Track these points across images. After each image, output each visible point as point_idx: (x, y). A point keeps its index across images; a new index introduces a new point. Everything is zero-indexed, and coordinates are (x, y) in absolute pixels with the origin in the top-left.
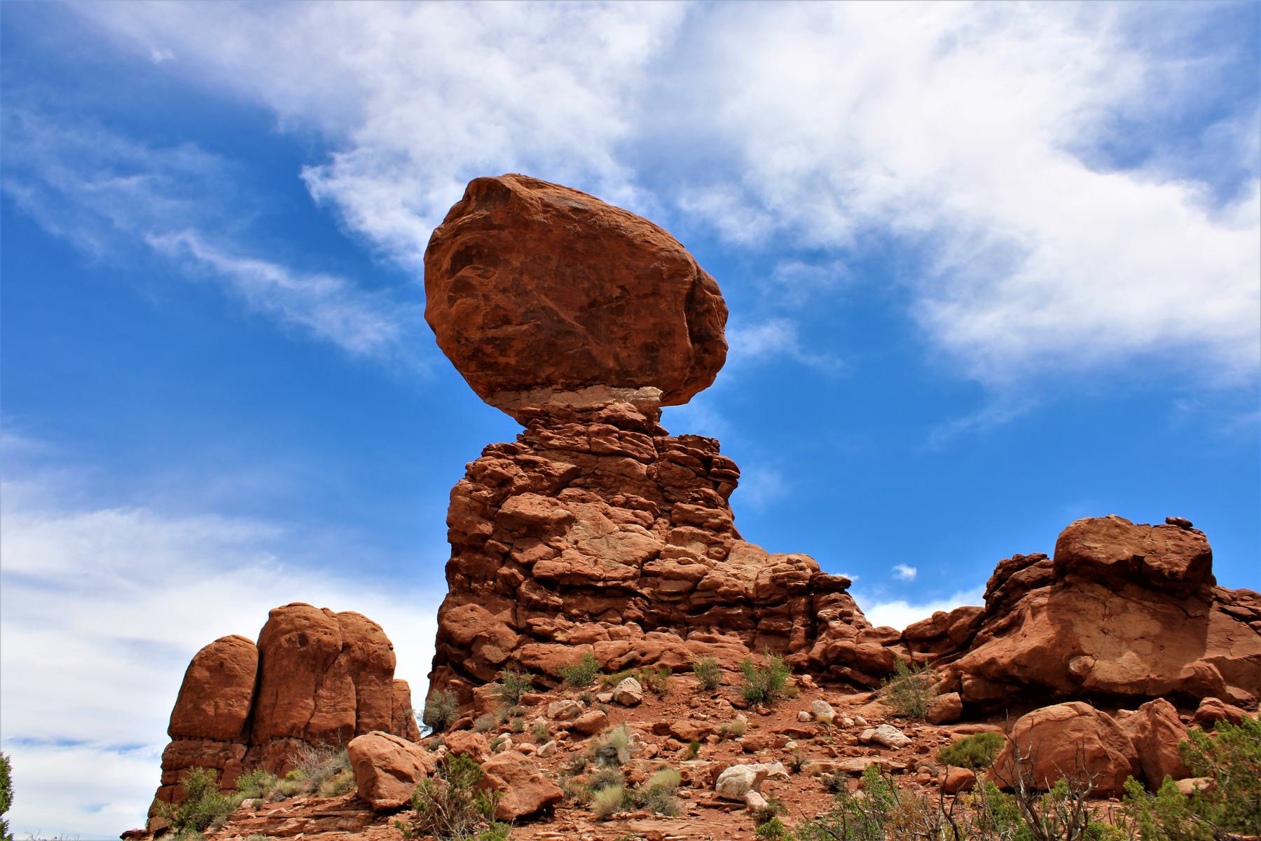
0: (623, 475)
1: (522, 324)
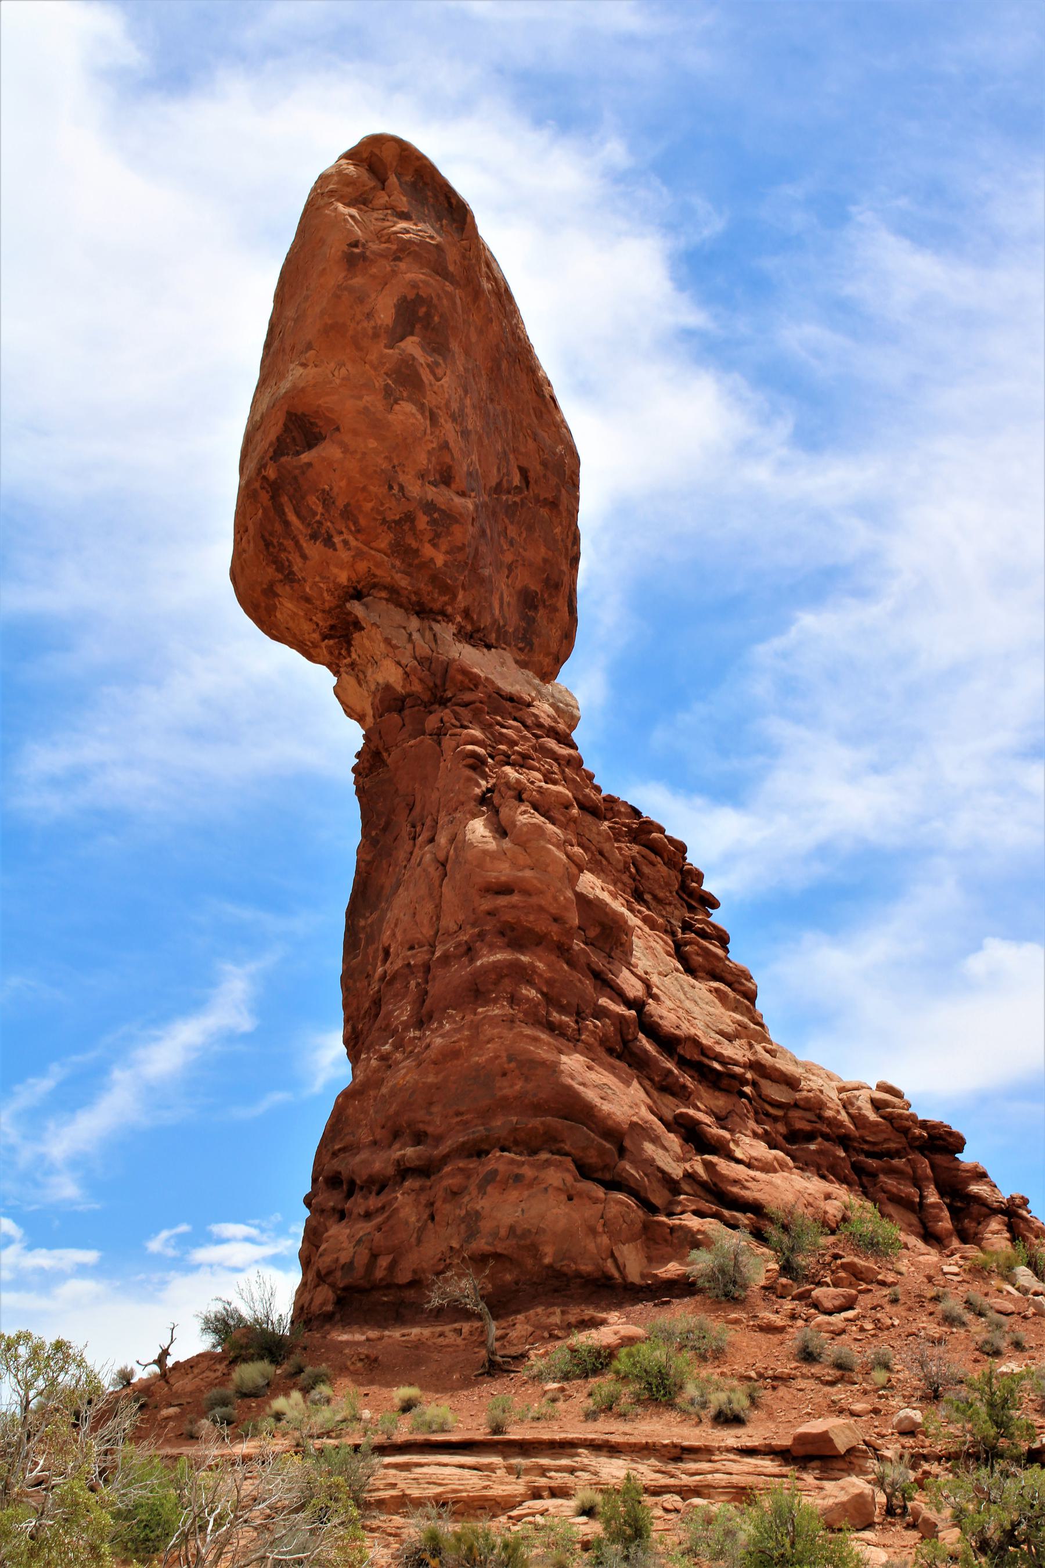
0: (601, 853)
1: (463, 494)
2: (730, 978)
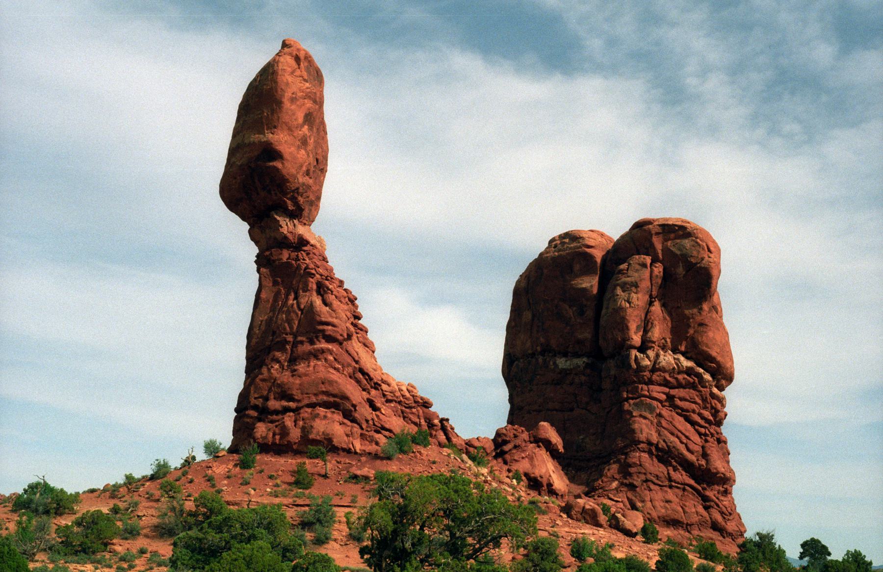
2: (368, 345)
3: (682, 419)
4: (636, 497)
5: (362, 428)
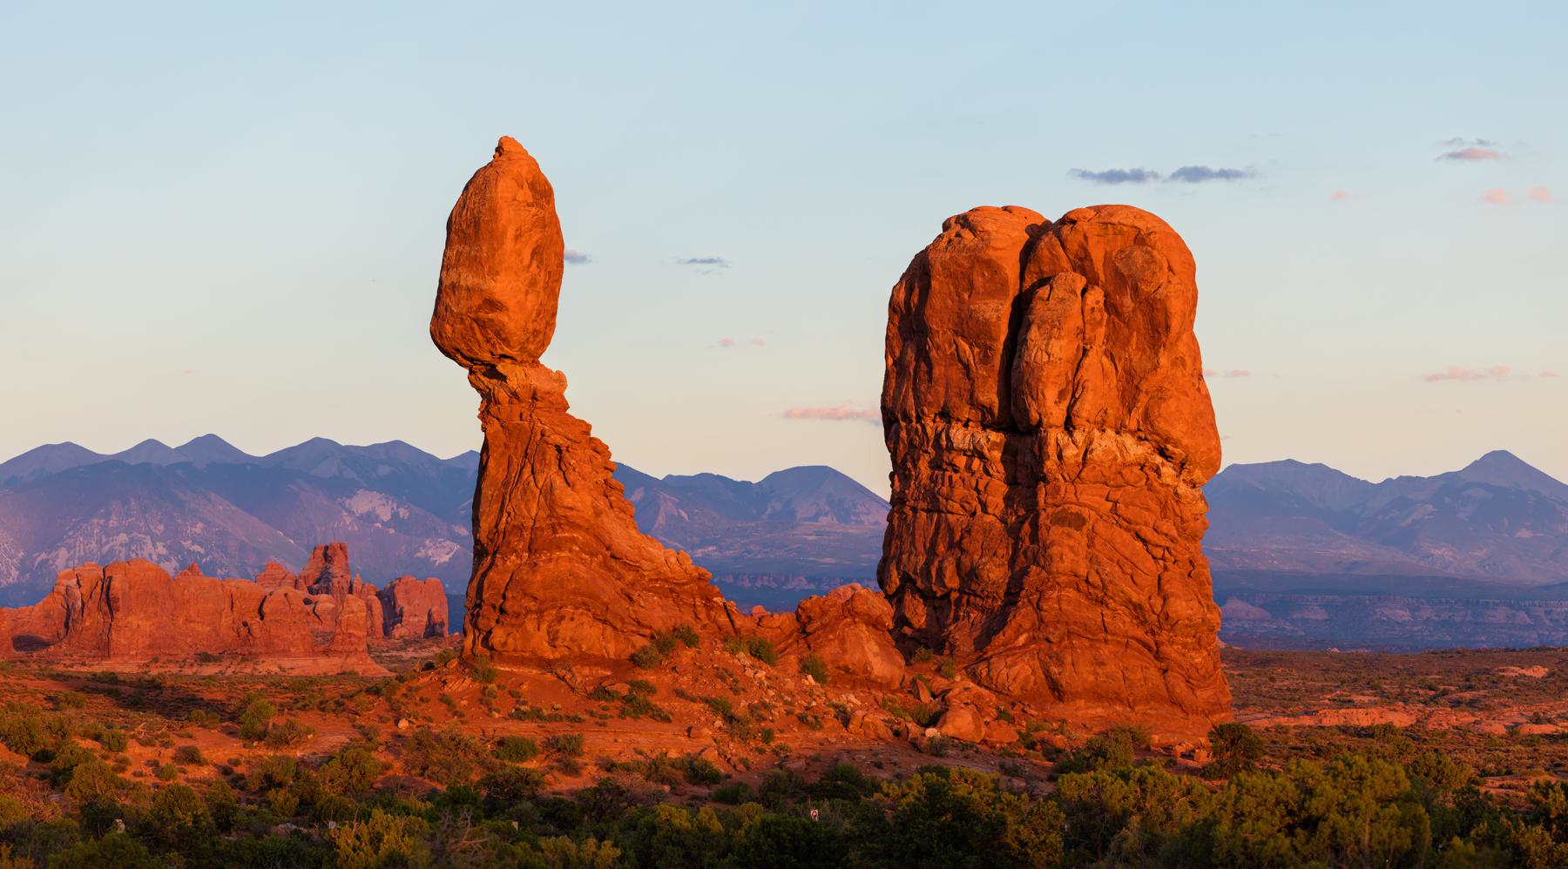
3: (1127, 536)
4: (1051, 658)
5: (615, 628)
